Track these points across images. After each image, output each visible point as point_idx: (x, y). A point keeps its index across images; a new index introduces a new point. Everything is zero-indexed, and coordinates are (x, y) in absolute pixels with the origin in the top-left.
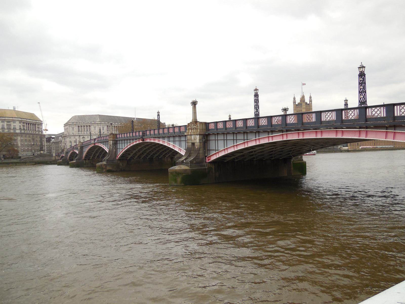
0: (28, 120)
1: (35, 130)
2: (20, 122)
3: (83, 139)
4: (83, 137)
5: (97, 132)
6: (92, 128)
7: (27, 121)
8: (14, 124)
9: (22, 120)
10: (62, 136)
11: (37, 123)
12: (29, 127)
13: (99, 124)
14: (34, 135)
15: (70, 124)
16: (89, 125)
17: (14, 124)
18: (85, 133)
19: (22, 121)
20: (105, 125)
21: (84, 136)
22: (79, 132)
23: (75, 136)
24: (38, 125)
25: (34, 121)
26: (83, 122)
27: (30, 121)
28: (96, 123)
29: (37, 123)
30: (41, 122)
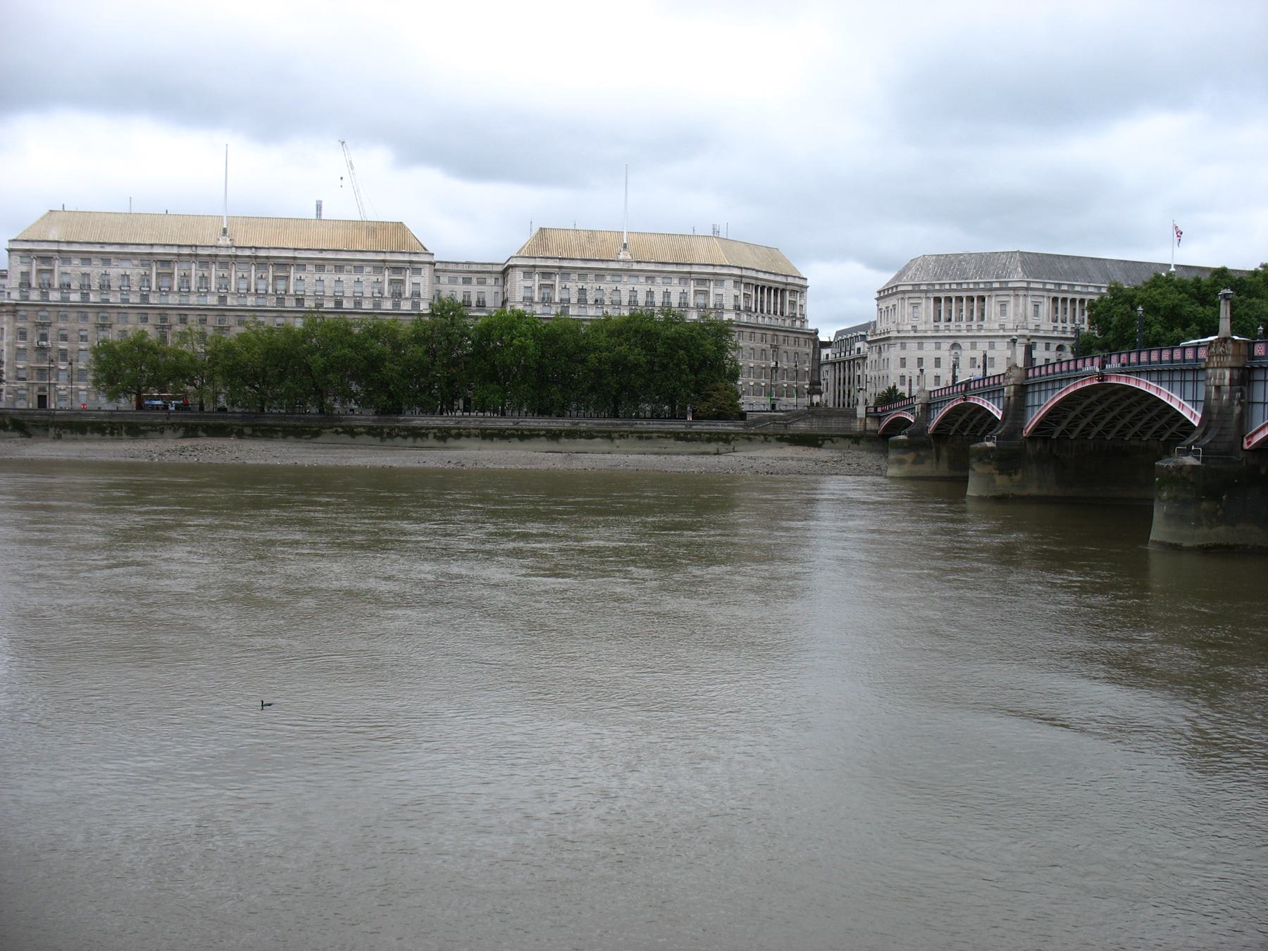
0: (761, 275)
1: (782, 314)
2: (739, 280)
3: (953, 352)
4: (954, 346)
5: (1010, 326)
6: (992, 307)
7: (756, 279)
8: (720, 291)
9: (745, 273)
10: (869, 339)
11: (788, 287)
12: (762, 302)
13: (1021, 293)
14: (777, 333)
15: (904, 292)
16: (981, 294)
17: (720, 291)
18: (963, 326)
19: (744, 280)
20: (1045, 294)
21: (959, 341)
22: (936, 324)
23: (924, 341)
24: (793, 292)
25: (779, 279)
26: (957, 284)
27: (767, 277)
28: (1010, 285)
29: (788, 287)
30: (801, 282)
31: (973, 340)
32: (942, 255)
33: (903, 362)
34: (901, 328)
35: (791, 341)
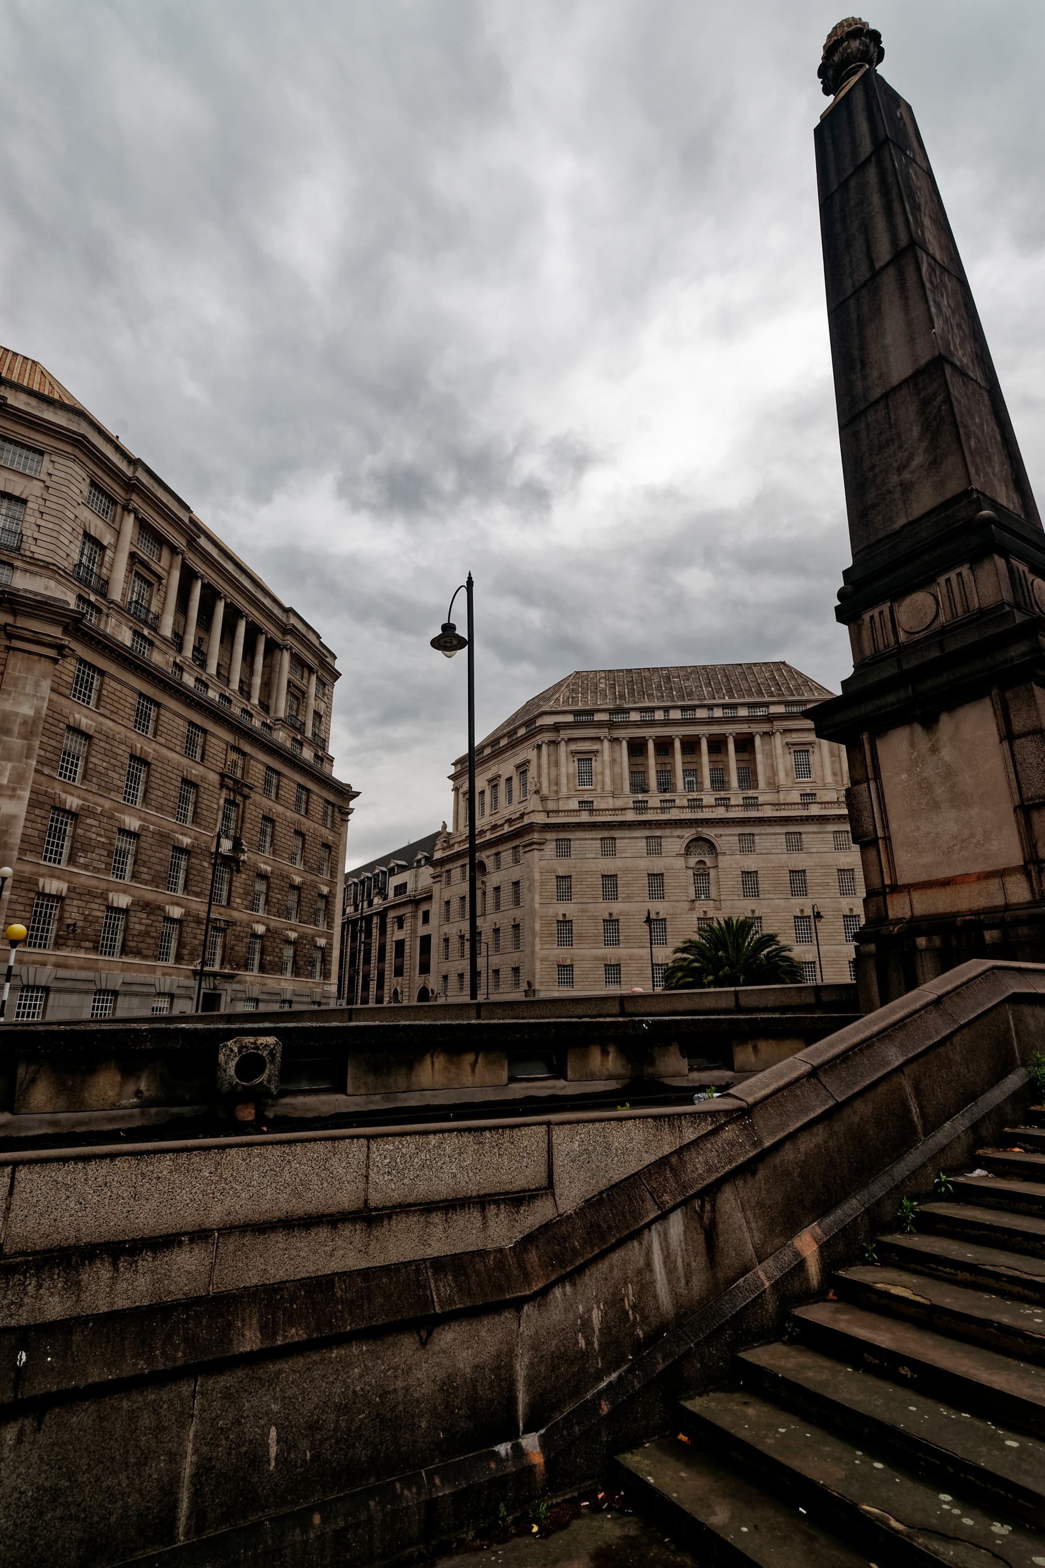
3: (693, 861)
5: (832, 796)
16: (744, 728)
21: (709, 832)
23: (617, 834)
31: (747, 830)
32: (622, 671)
33: (564, 885)
34: (551, 805)
35: (289, 791)
